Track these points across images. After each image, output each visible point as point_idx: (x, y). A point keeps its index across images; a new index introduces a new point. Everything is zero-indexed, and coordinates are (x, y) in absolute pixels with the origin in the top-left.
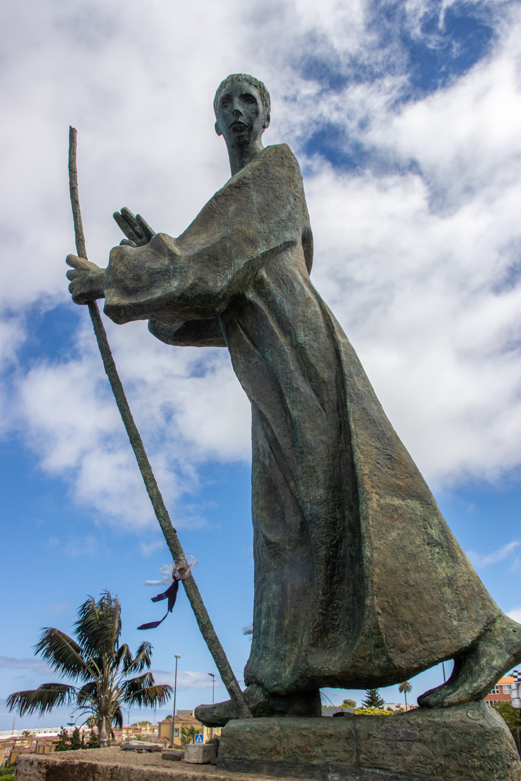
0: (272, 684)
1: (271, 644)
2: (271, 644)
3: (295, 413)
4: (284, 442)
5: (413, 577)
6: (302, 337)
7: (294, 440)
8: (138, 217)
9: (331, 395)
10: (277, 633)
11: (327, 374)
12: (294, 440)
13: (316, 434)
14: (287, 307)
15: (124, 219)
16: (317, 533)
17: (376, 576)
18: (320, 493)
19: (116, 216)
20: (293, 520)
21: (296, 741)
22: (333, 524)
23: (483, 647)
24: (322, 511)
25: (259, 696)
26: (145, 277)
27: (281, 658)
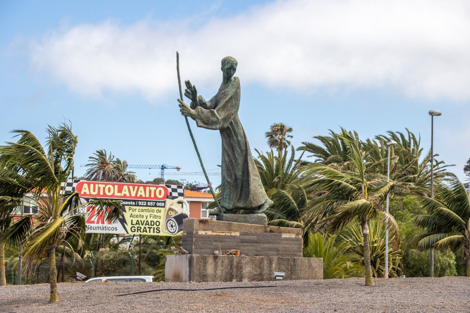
0: (228, 208)
1: (227, 201)
2: (227, 201)
3: (237, 156)
4: (233, 161)
5: (257, 192)
6: (240, 139)
7: (236, 162)
8: (194, 87)
9: (244, 153)
10: (229, 199)
11: (244, 148)
12: (236, 162)
13: (240, 160)
14: (237, 130)
15: (188, 83)
16: (239, 182)
17: (252, 192)
18: (240, 174)
19: (186, 82)
20: (233, 177)
21: (236, 217)
22: (242, 180)
23: (265, 204)
24: (240, 177)
25: (224, 210)
26: (210, 122)
27: (229, 203)
